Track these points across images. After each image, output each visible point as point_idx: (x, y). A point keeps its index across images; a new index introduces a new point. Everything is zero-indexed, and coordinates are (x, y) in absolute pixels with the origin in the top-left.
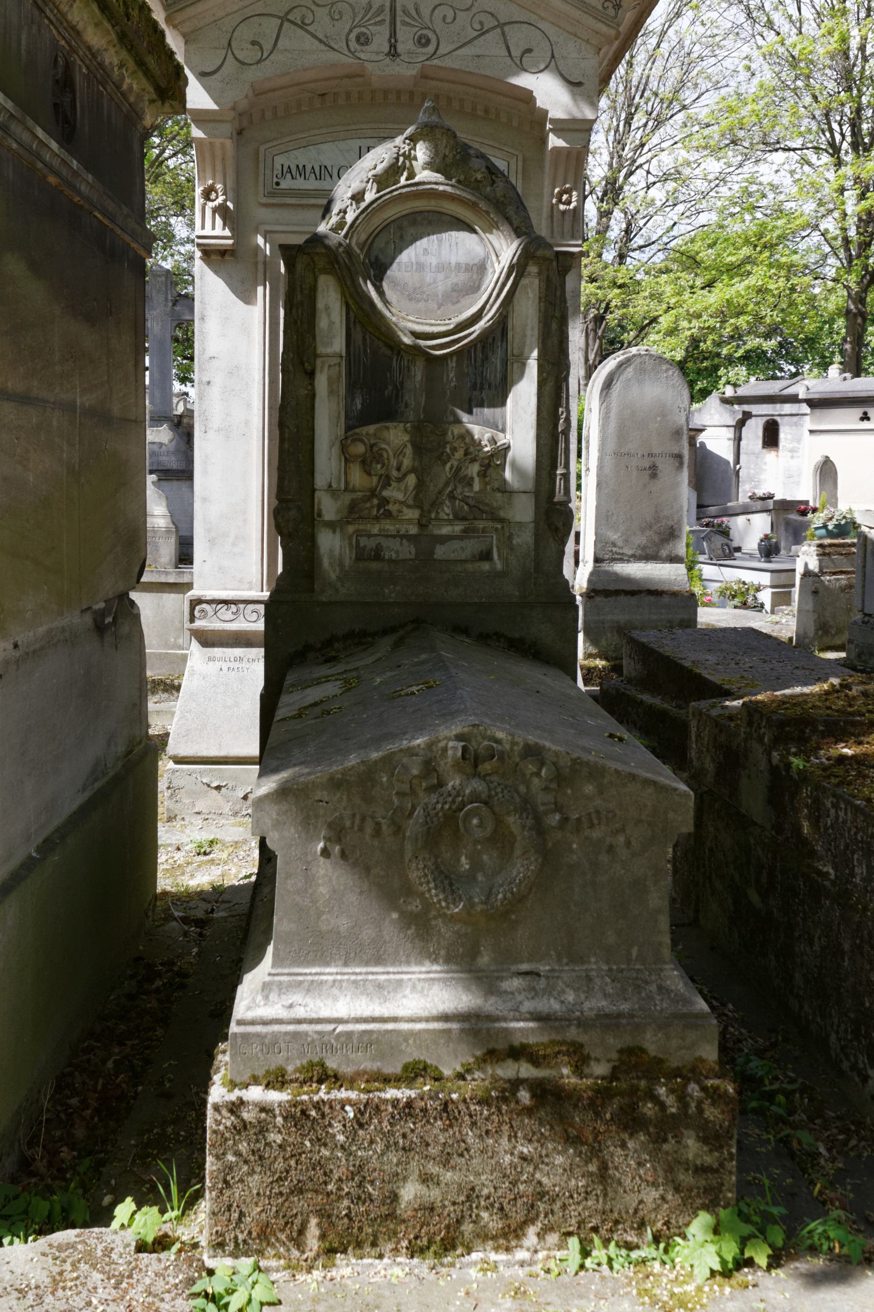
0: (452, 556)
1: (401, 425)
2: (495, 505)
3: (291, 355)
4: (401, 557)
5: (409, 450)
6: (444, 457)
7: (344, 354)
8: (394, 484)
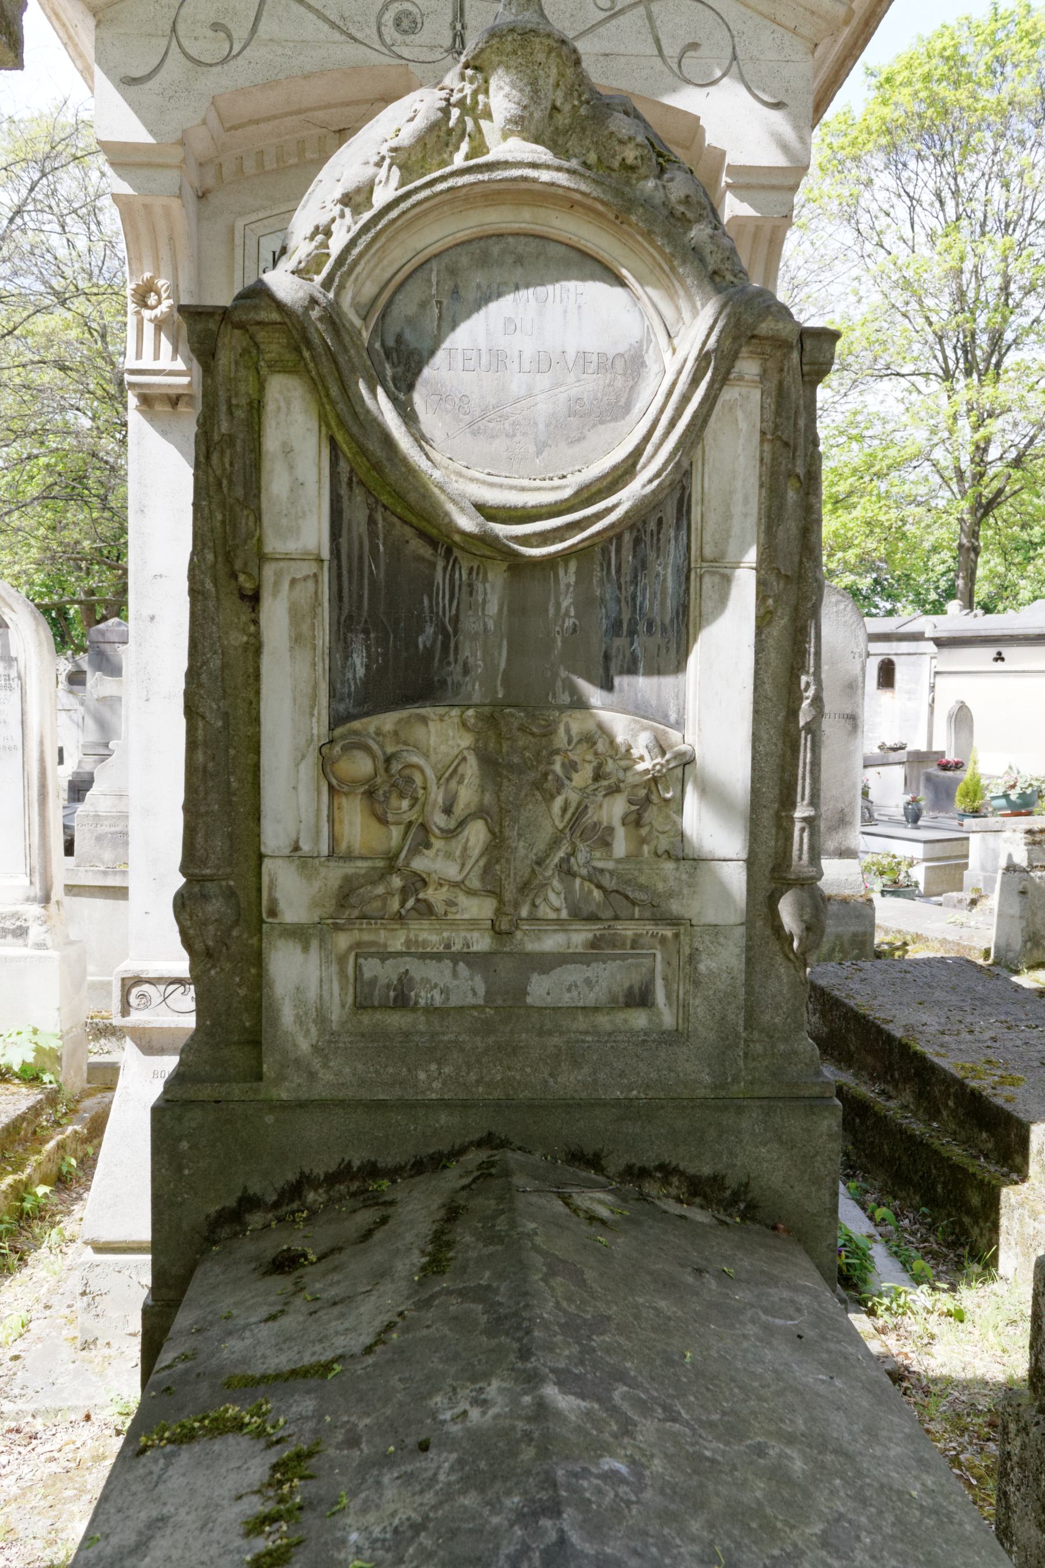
0: (567, 999)
1: (455, 712)
2: (660, 887)
3: (210, 557)
4: (455, 1001)
5: (471, 768)
6: (550, 784)
7: (326, 554)
8: (438, 844)
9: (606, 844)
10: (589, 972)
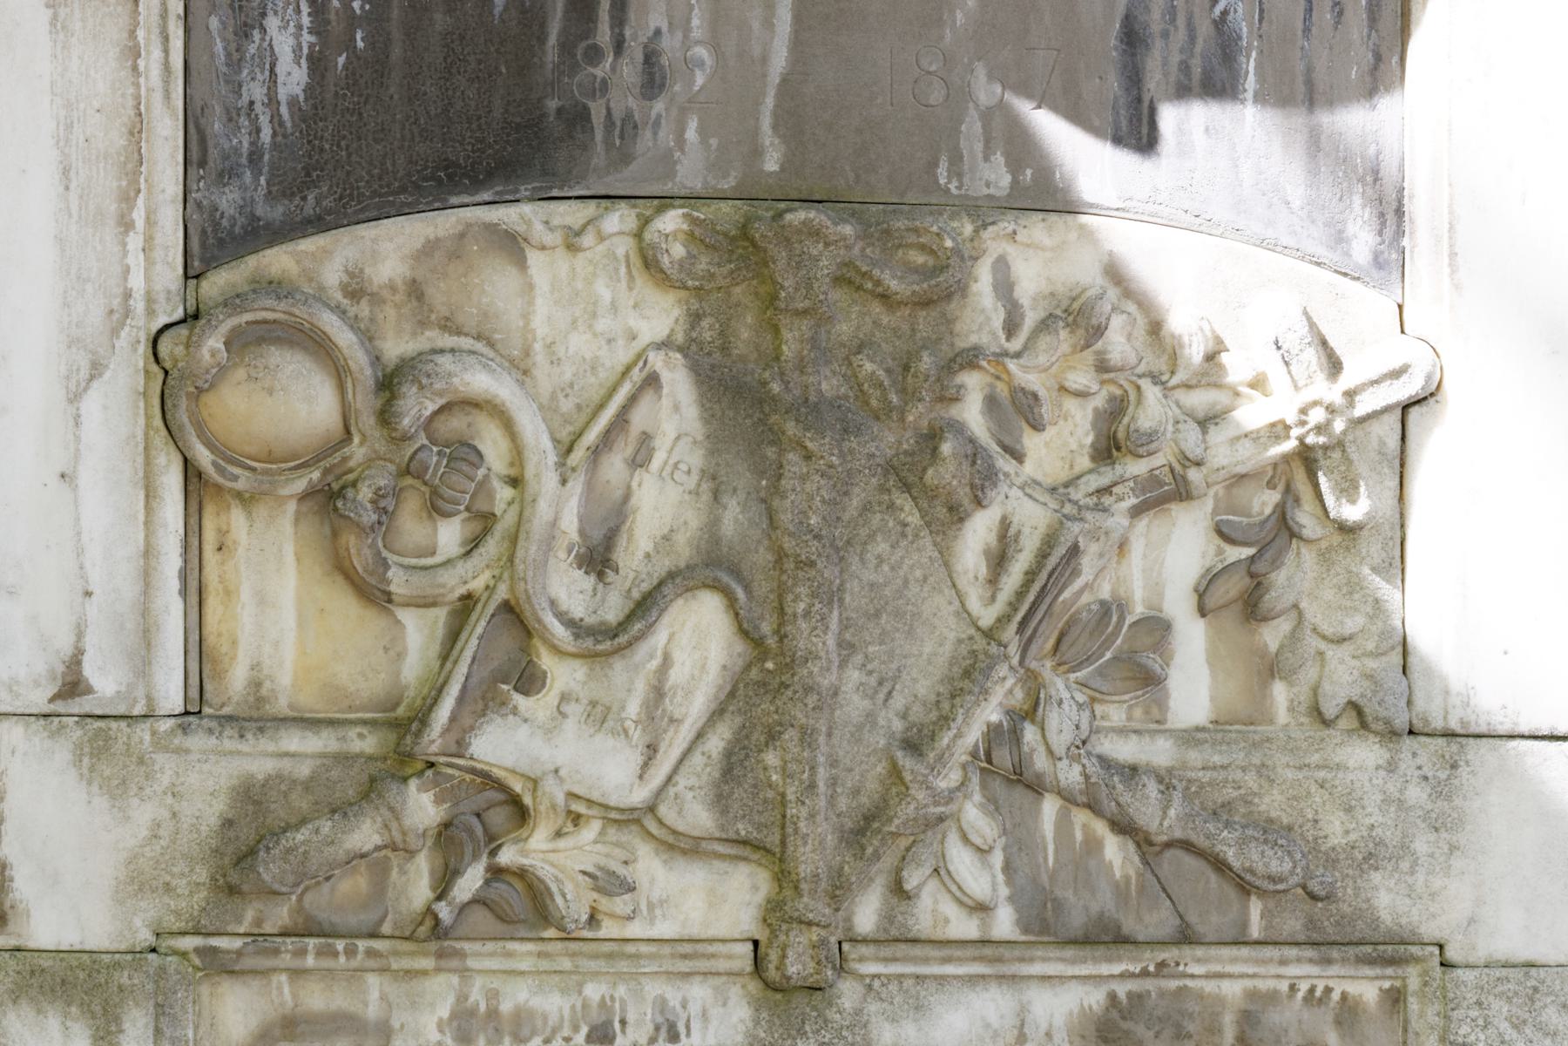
1: (619, 220)
2: (1335, 829)
5: (676, 414)
6: (948, 471)
8: (563, 674)
9: (1145, 679)
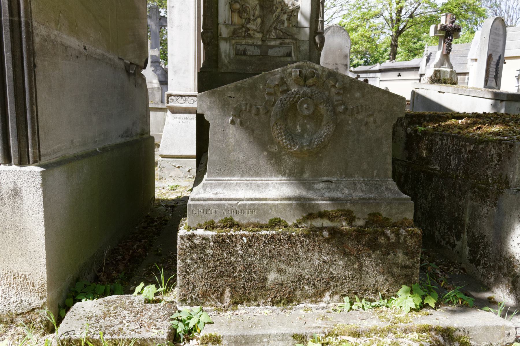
0: (275, 54)
2: (293, 32)
4: (254, 54)
5: (258, 8)
6: (273, 11)
8: (252, 22)
9: (283, 23)
10: (280, 49)
